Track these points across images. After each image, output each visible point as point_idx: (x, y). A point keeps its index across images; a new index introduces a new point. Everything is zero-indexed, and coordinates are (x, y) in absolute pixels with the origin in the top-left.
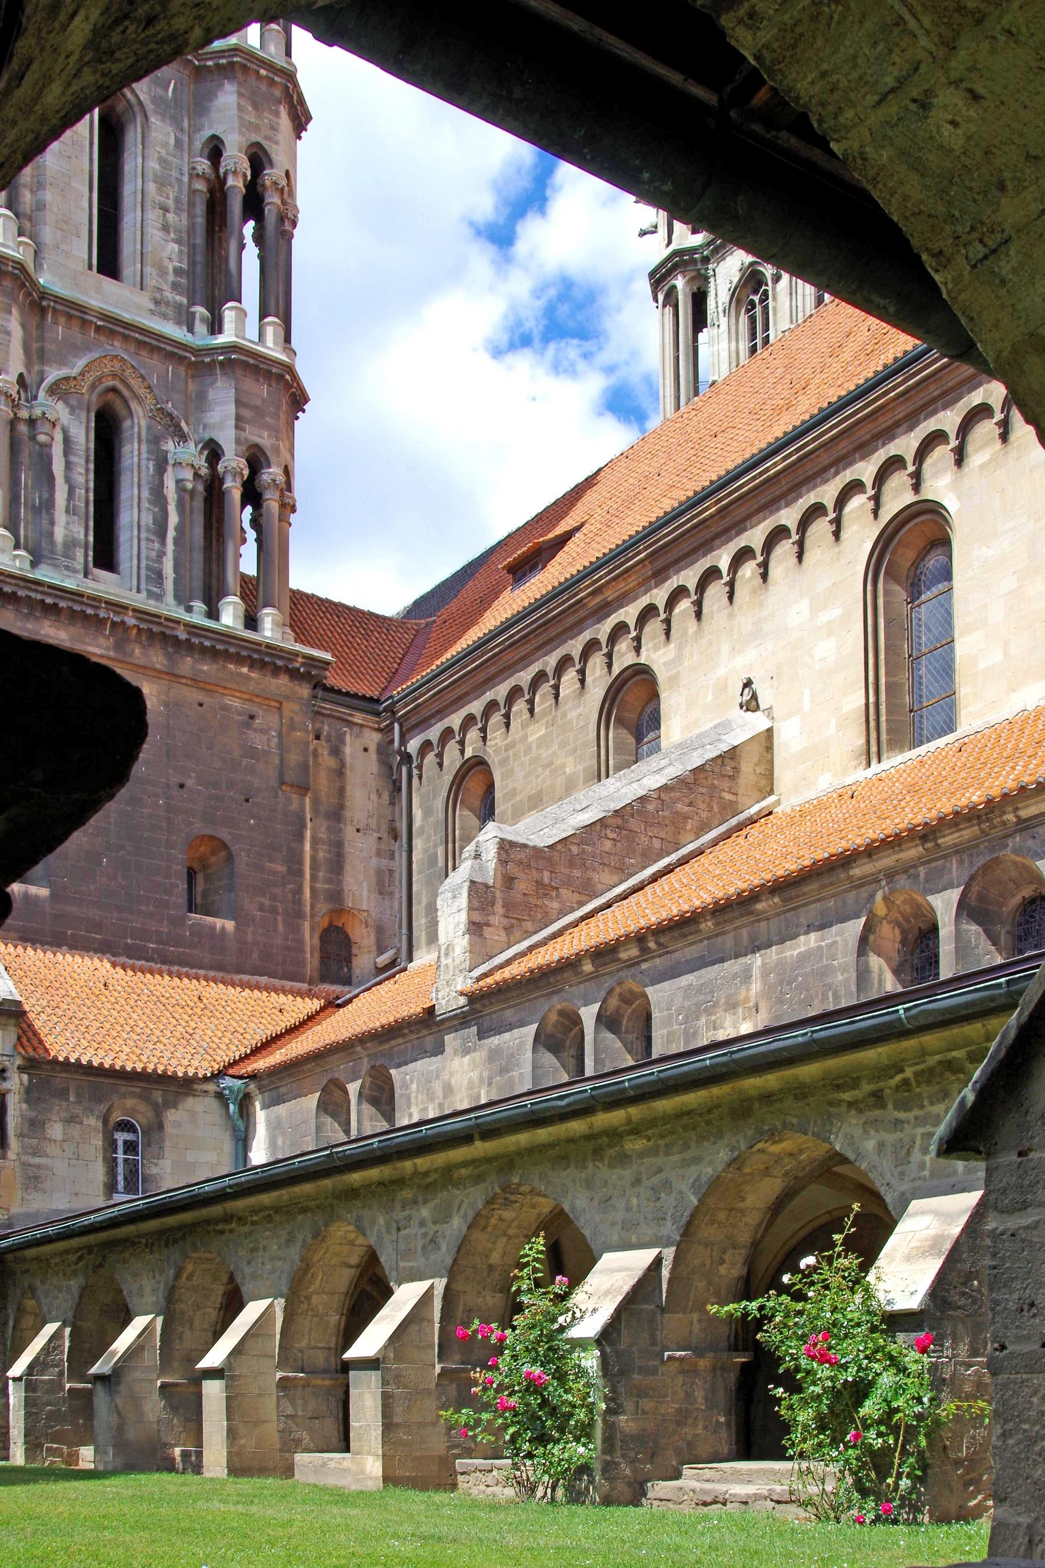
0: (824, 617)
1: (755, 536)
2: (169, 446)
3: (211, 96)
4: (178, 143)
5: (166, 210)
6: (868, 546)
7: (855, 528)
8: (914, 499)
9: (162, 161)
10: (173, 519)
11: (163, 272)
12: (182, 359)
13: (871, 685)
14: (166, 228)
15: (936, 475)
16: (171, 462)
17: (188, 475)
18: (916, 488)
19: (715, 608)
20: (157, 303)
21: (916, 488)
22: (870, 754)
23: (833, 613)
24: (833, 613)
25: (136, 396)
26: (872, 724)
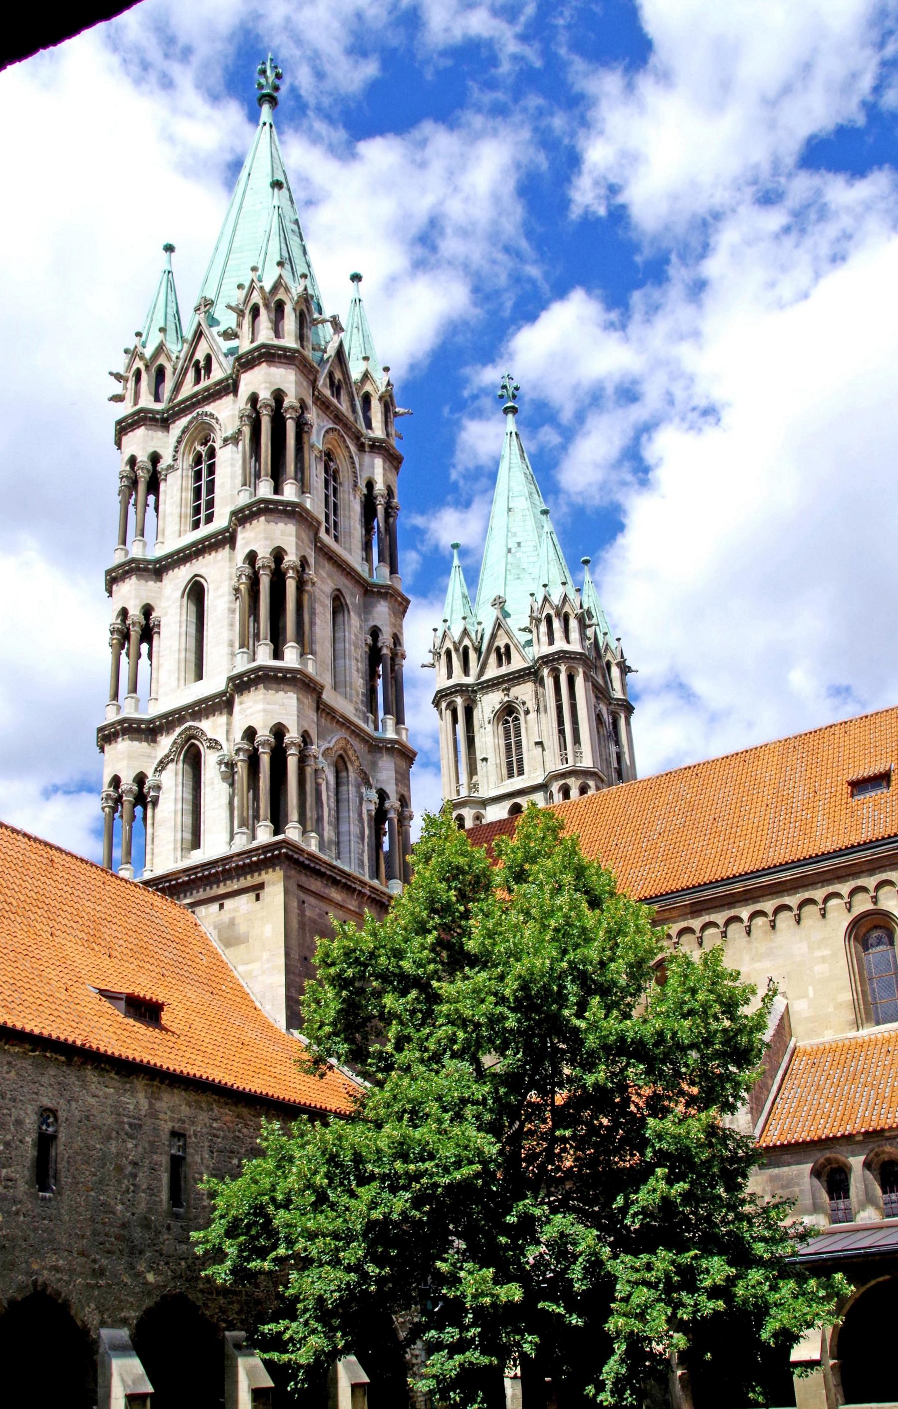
0: (818, 953)
1: (768, 906)
2: (363, 790)
3: (373, 606)
4: (361, 627)
5: (357, 661)
6: (846, 924)
7: (835, 914)
8: (870, 906)
9: (356, 635)
10: (367, 832)
11: (358, 695)
12: (368, 741)
13: (854, 991)
14: (358, 670)
15: (886, 899)
16: (365, 799)
17: (373, 807)
18: (875, 903)
19: (737, 936)
20: (356, 710)
21: (875, 903)
22: (858, 1026)
23: (826, 952)
24: (826, 952)
25: (351, 761)
26: (857, 1009)
